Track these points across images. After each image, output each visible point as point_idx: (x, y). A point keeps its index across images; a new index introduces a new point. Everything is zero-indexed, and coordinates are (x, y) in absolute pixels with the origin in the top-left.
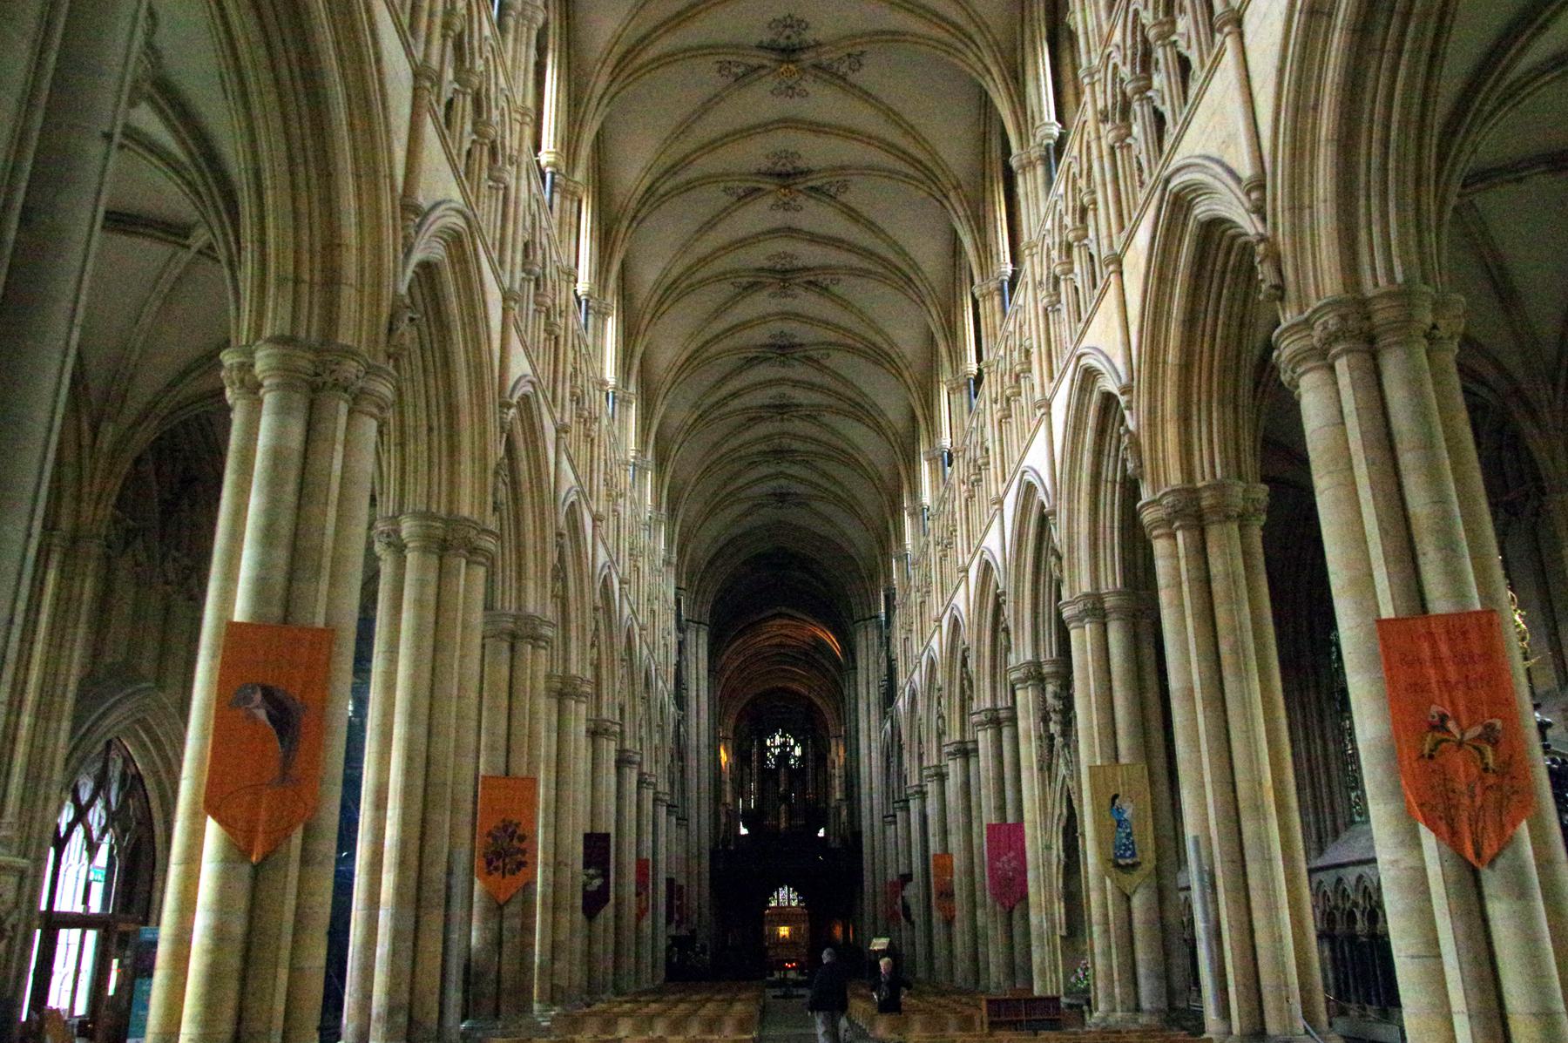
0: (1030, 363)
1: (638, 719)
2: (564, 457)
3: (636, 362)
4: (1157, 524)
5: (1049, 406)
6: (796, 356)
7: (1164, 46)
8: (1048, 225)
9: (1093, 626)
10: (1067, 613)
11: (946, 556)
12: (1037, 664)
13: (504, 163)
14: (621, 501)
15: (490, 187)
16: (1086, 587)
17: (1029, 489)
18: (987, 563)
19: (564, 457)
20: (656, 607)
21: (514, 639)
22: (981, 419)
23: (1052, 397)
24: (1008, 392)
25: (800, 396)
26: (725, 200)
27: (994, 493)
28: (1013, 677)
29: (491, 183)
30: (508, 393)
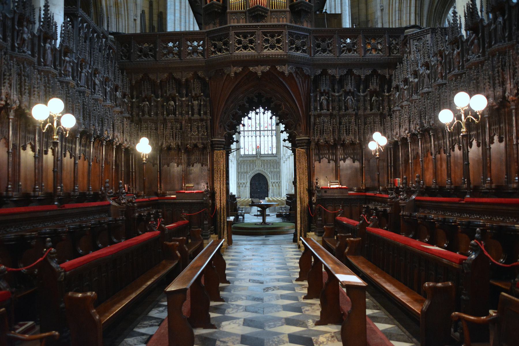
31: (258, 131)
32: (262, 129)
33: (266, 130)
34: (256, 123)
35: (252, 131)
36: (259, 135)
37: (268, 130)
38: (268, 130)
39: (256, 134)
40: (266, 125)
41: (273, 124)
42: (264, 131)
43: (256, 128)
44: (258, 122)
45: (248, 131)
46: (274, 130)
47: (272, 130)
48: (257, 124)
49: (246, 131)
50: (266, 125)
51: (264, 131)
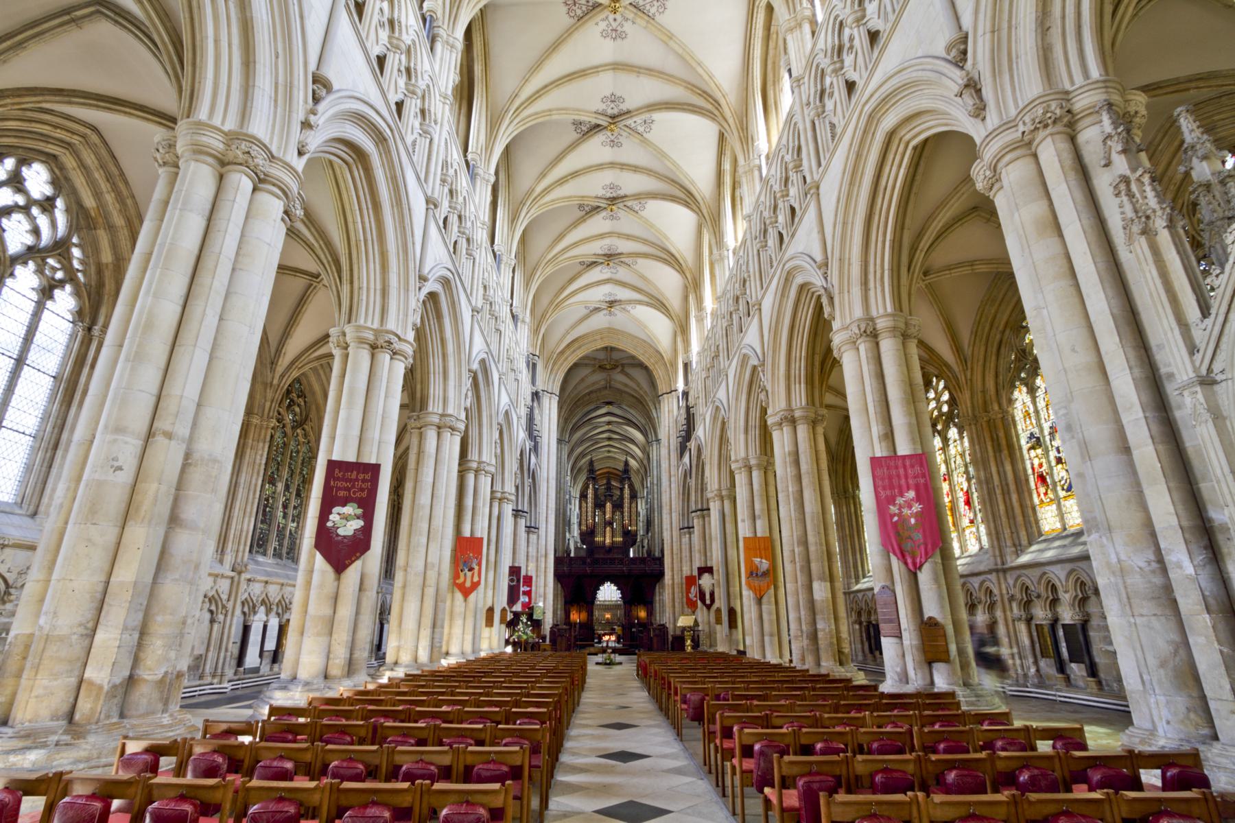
0: (801, 160)
1: (464, 391)
2: (476, 326)
4: (844, 343)
7: (859, 26)
8: (741, 254)
9: (868, 344)
10: (770, 421)
12: (790, 409)
16: (858, 312)
17: (745, 358)
18: (717, 407)
19: (476, 326)
21: (374, 347)
23: (763, 297)
24: (732, 309)
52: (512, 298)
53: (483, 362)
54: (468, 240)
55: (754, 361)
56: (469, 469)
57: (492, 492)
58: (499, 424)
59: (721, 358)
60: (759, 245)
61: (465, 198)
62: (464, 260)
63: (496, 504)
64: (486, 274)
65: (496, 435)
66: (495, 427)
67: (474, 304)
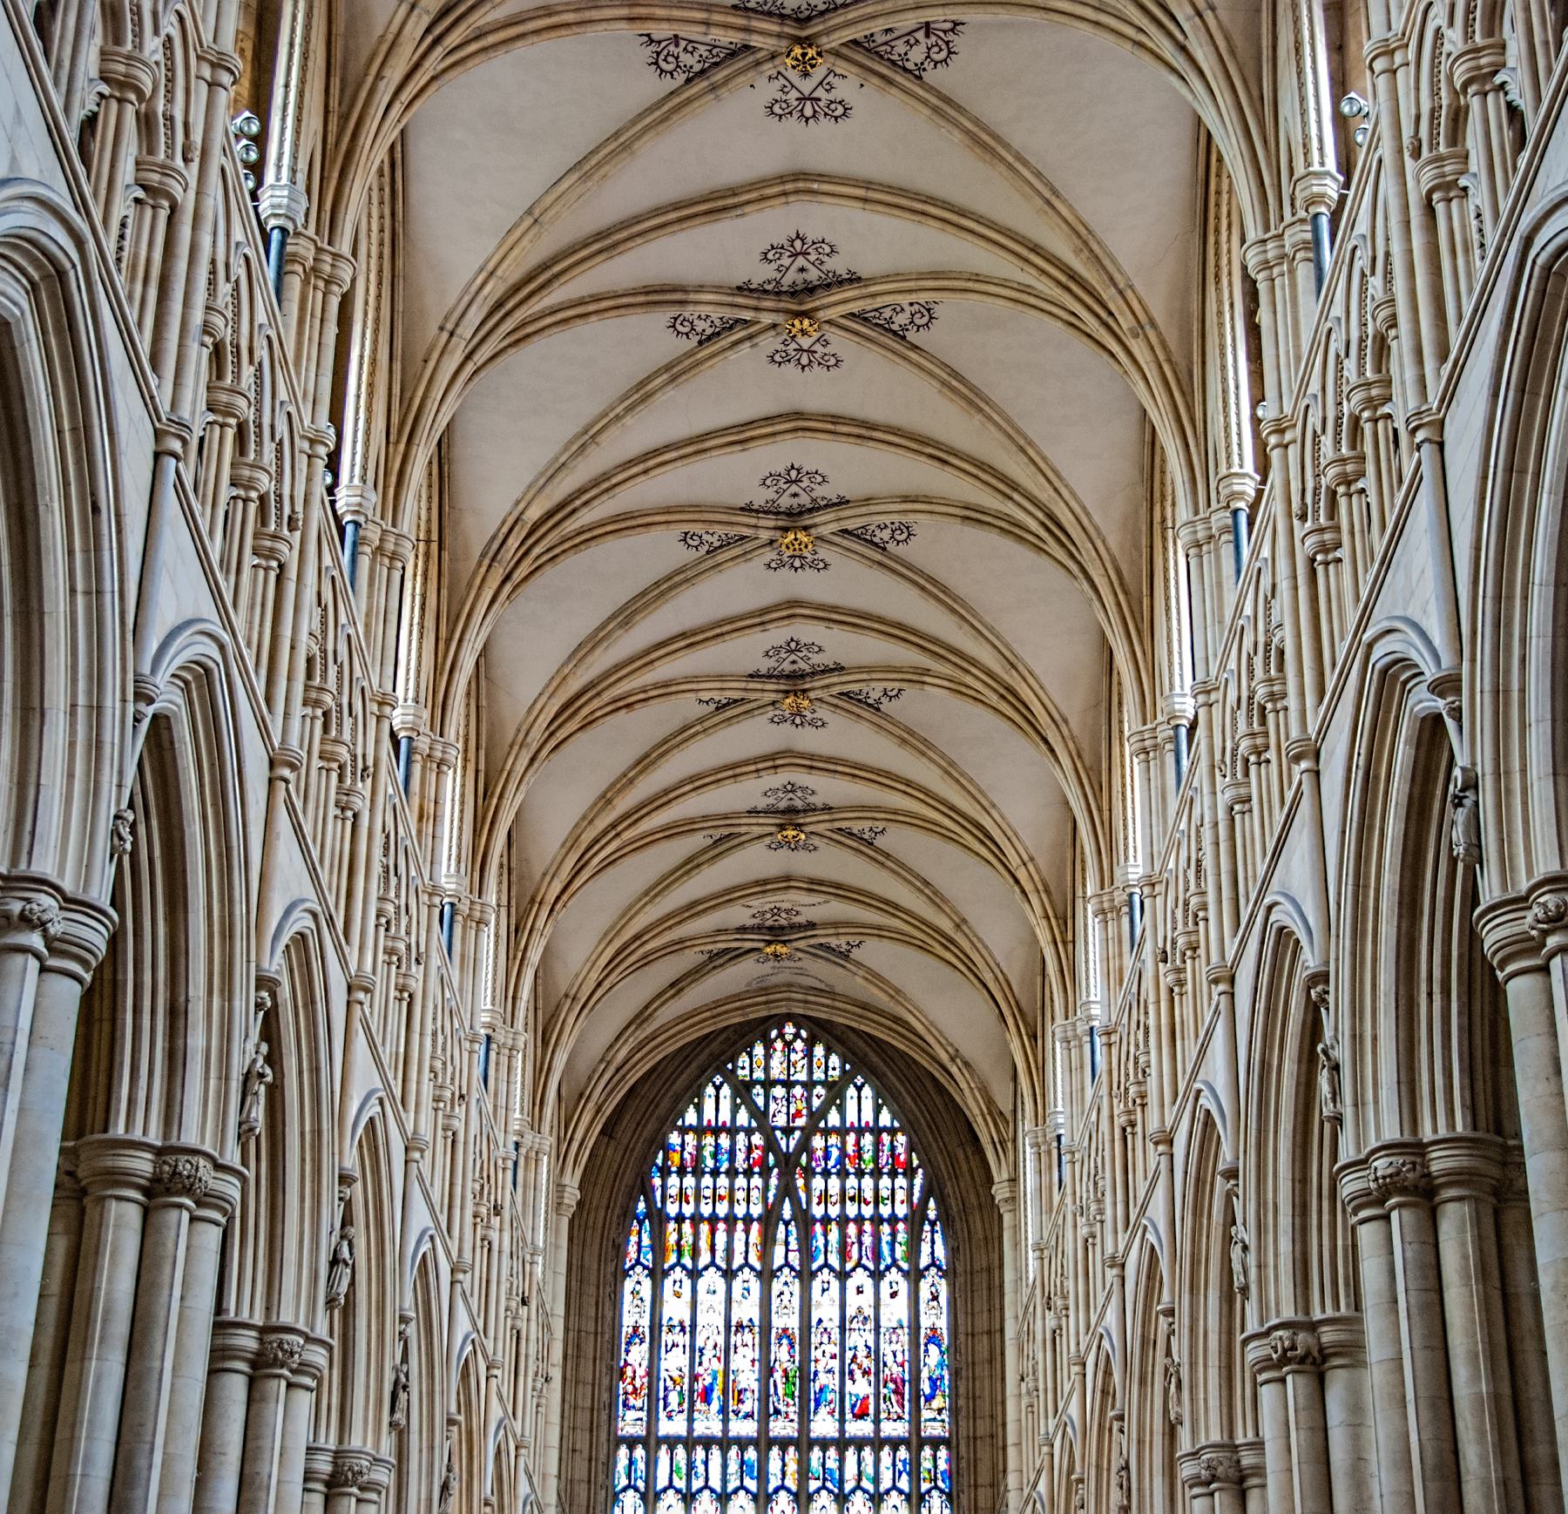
3: (422, 455)
5: (1441, 423)
6: (824, 531)
11: (1181, 983)
13: (170, 156)
14: (364, 788)
15: (101, 95)
20: (458, 1125)
22: (1266, 582)
25: (837, 644)
26: (653, 86)
27: (1295, 733)
28: (1346, 1191)
29: (106, 90)
30: (153, 646)
31: (784, 1444)
32: (824, 1425)
33: (860, 1443)
34: (767, 1371)
35: (725, 1443)
36: (791, 1483)
37: (877, 1443)
38: (877, 1443)
39: (763, 1477)
40: (861, 1387)
41: (926, 1387)
42: (842, 1443)
43: (766, 1414)
44: (781, 1353)
45: (690, 1442)
46: (935, 1443)
47: (915, 1442)
48: (778, 1376)
49: (672, 1442)
50: (861, 1387)
51: (842, 1443)
52: (336, 418)
53: (199, 679)
54: (146, 123)
55: (1422, 701)
56: (119, 1178)
57: (221, 1326)
58: (265, 982)
59: (1292, 702)
60: (1428, 177)
61: (168, 42)
62: (122, 207)
63: (235, 1387)
64: (224, 289)
65: (247, 1049)
66: (245, 998)
67: (164, 407)
